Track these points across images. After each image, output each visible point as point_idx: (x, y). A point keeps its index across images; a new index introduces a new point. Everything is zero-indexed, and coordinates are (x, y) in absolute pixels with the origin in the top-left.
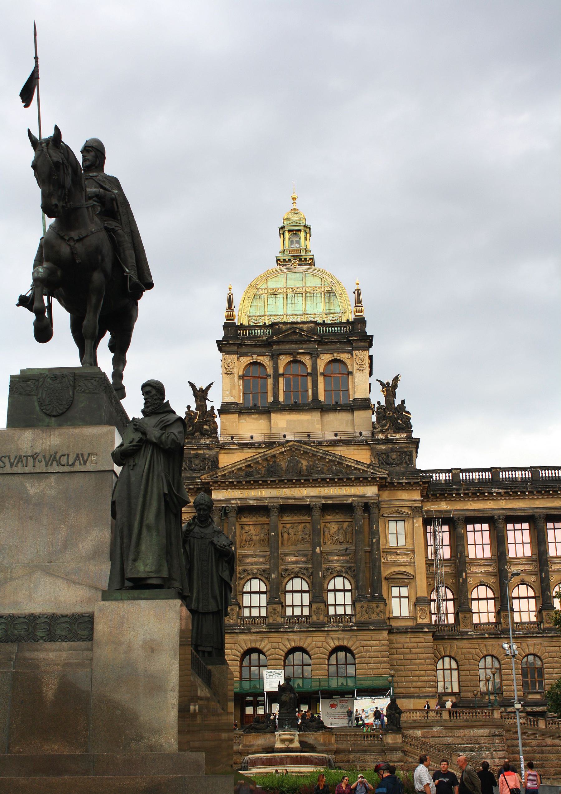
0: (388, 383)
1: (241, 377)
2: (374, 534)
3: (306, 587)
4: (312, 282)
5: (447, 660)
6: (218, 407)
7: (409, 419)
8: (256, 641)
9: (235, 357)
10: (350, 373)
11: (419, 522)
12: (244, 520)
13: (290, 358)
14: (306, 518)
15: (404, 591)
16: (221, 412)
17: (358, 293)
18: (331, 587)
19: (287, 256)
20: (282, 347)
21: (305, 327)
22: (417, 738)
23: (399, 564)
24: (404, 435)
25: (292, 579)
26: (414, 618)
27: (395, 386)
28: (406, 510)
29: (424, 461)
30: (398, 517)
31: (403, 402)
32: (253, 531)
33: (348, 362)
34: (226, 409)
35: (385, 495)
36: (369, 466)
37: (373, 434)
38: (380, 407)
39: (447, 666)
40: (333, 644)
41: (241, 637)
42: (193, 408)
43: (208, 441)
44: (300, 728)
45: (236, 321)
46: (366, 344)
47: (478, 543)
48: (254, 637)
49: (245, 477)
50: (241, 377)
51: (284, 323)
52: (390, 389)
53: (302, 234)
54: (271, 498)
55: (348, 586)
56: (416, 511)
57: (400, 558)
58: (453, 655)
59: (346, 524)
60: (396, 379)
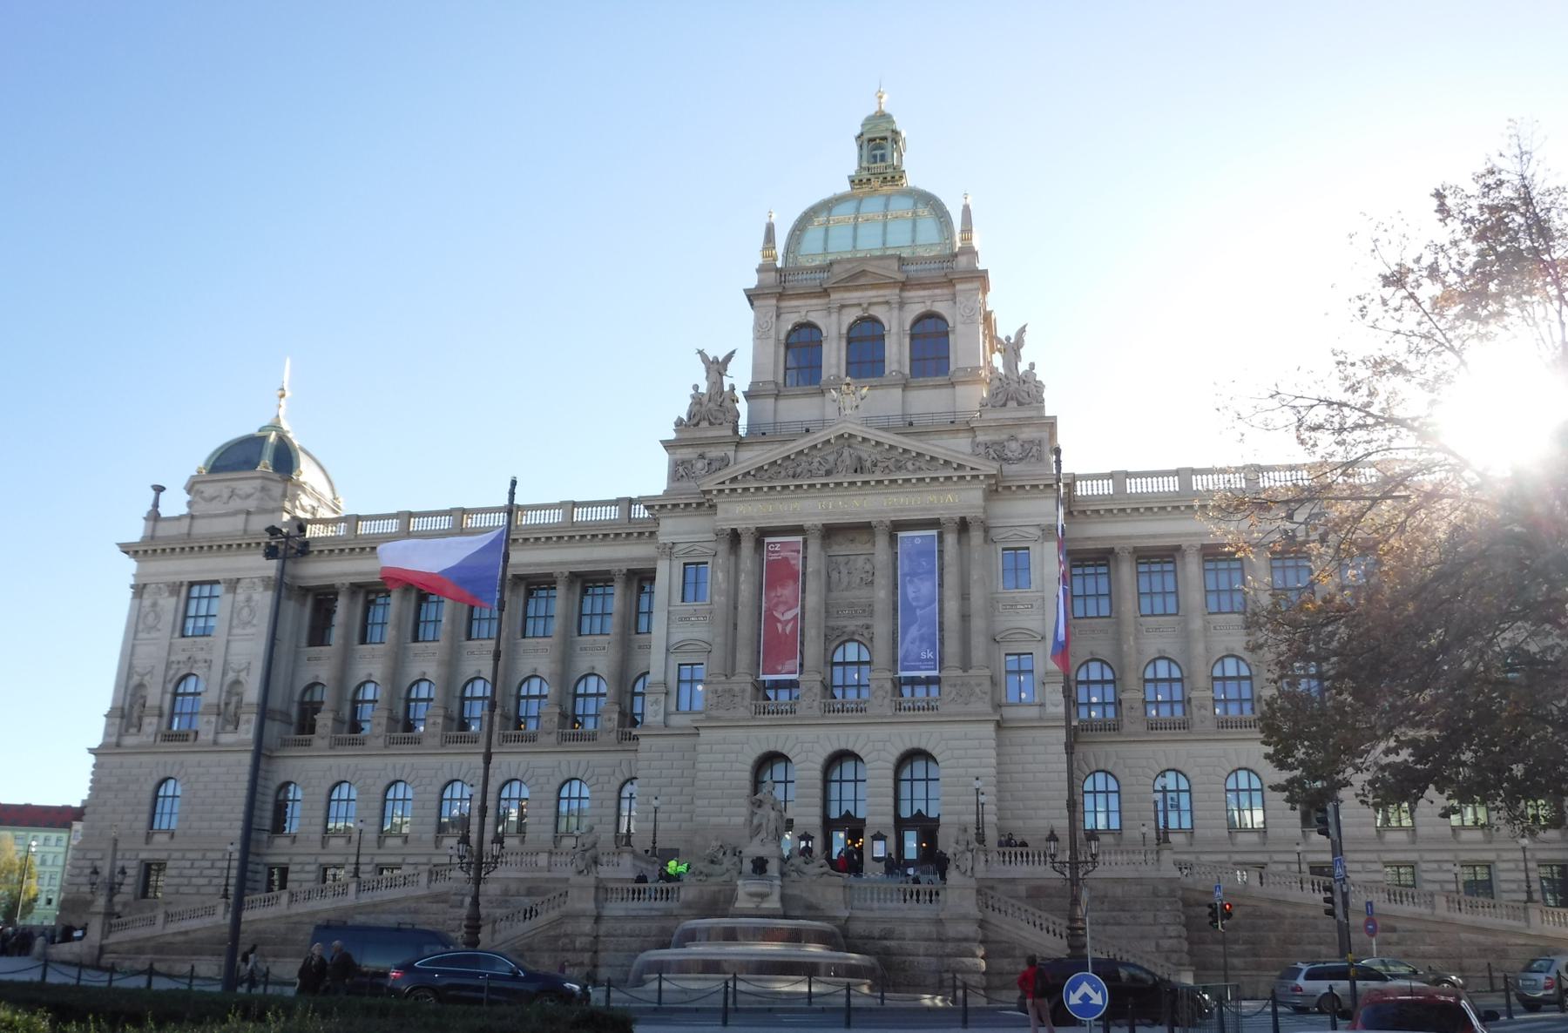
0: (1008, 339)
5: (1100, 777)
16: (747, 396)
17: (966, 211)
19: (865, 175)
20: (847, 295)
25: (844, 643)
26: (1042, 705)
28: (1031, 530)
31: (1032, 366)
39: (1100, 786)
42: (703, 389)
46: (976, 285)
52: (1012, 350)
53: (889, 144)
58: (1109, 768)
60: (1023, 330)
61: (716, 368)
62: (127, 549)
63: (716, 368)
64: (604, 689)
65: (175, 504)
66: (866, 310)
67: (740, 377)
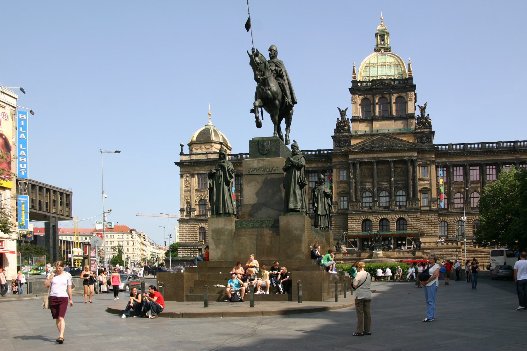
1: (360, 105)
2: (414, 172)
3: (387, 194)
4: (390, 60)
6: (350, 118)
7: (431, 122)
9: (357, 96)
10: (407, 102)
11: (433, 167)
12: (362, 167)
13: (380, 96)
14: (387, 166)
15: (427, 196)
17: (409, 65)
18: (398, 194)
21: (387, 82)
22: (427, 253)
23: (424, 184)
24: (428, 130)
26: (430, 207)
27: (425, 108)
29: (436, 141)
30: (424, 165)
31: (428, 115)
32: (366, 172)
33: (405, 97)
34: (355, 120)
35: (420, 156)
36: (413, 143)
37: (416, 129)
38: (419, 118)
40: (398, 216)
42: (340, 119)
43: (346, 134)
45: (357, 79)
47: (458, 175)
49: (362, 150)
50: (360, 105)
51: (378, 80)
52: (423, 110)
53: (386, 37)
54: (374, 158)
55: (404, 194)
56: (432, 163)
57: (425, 182)
59: (404, 168)
60: (426, 105)
61: (343, 113)
62: (177, 164)
63: (343, 113)
65: (186, 151)
66: (382, 95)
67: (349, 116)
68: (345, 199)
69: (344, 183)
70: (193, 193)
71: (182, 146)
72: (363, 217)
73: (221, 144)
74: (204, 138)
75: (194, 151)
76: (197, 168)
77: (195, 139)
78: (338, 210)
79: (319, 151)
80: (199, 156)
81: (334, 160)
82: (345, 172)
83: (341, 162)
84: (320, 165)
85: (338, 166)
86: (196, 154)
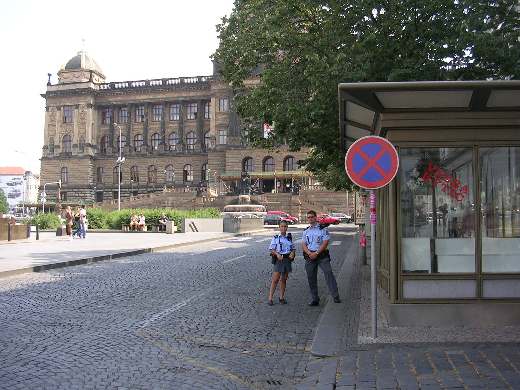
8: (249, 153)
41: (242, 151)
44: (252, 194)
48: (248, 151)
62: (42, 95)
64: (196, 136)
65: (55, 81)
68: (225, 132)
69: (224, 114)
70: (58, 128)
71: (50, 75)
72: (244, 154)
73: (91, 72)
74: (74, 65)
75: (63, 81)
76: (64, 100)
77: (64, 68)
78: (216, 146)
79: (200, 78)
80: (67, 86)
81: (213, 87)
82: (226, 101)
83: (222, 89)
84: (199, 94)
85: (218, 95)
86: (64, 84)
